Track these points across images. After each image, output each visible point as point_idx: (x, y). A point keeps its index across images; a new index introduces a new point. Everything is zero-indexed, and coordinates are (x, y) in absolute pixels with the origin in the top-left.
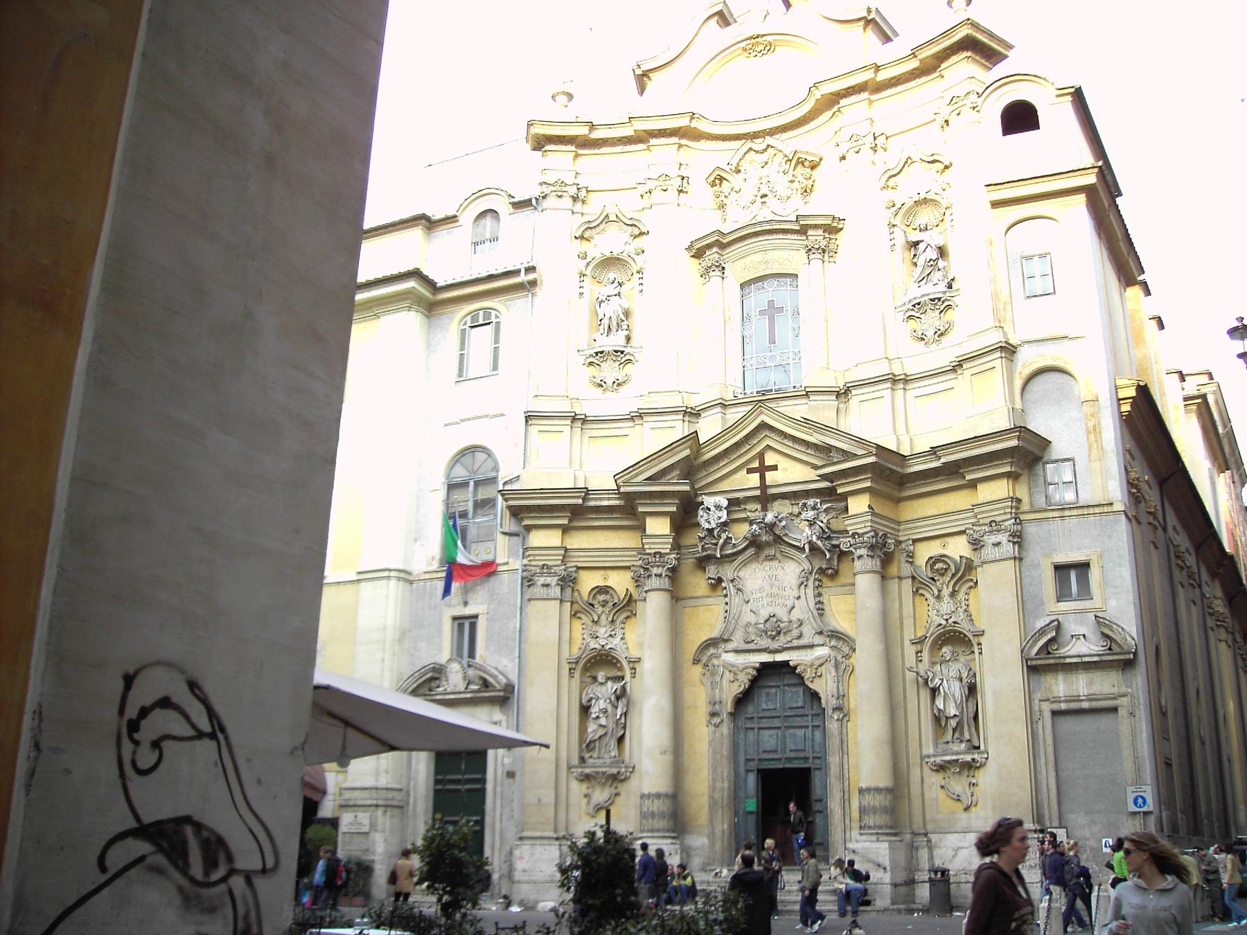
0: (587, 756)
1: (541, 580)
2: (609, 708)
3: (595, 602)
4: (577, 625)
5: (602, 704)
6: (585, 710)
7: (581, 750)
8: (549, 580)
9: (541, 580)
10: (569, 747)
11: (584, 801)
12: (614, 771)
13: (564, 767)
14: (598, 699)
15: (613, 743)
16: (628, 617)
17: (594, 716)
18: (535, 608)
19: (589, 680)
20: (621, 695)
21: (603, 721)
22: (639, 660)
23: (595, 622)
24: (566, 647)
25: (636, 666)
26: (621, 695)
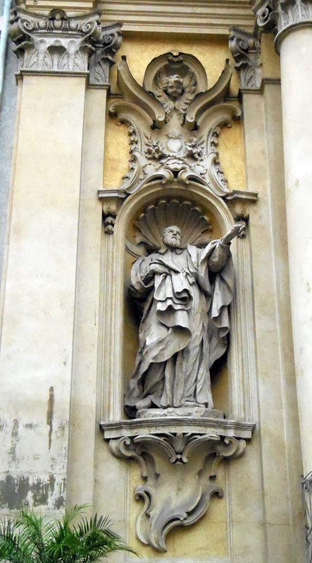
0: (140, 404)
1: (50, 41)
2: (194, 292)
3: (157, 92)
4: (120, 140)
5: (180, 283)
6: (137, 304)
7: (127, 393)
8: (64, 42)
9: (50, 41)
10: (98, 387)
11: (135, 512)
12: (212, 433)
13: (90, 428)
14: (170, 271)
15: (204, 374)
16: (224, 125)
17: (161, 307)
18: (33, 91)
19: (140, 251)
20: (217, 270)
21: (181, 319)
22: (253, 200)
23: (156, 127)
24: (96, 170)
25: (250, 211)
26: (217, 270)
